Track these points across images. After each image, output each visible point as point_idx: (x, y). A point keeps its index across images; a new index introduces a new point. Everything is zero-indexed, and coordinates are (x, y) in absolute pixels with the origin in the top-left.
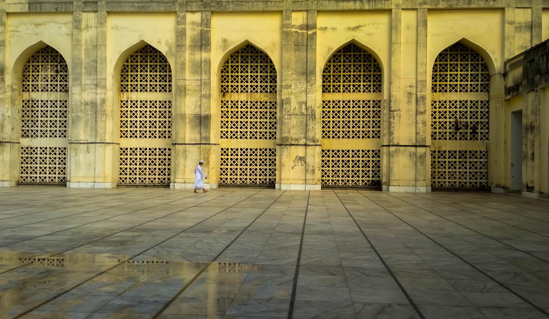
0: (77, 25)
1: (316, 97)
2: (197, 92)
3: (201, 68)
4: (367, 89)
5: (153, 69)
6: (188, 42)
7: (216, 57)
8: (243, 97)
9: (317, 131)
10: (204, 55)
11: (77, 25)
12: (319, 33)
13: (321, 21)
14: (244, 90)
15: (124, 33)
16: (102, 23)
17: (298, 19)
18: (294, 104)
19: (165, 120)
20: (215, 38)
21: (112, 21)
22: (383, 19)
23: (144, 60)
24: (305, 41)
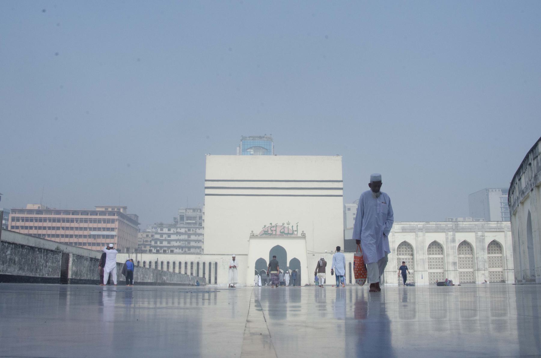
0: (417, 236)
1: (486, 256)
2: (451, 254)
3: (453, 248)
4: (498, 253)
5: (436, 248)
6: (449, 240)
7: (457, 244)
8: (462, 256)
9: (487, 266)
10: (454, 244)
11: (417, 236)
12: (486, 238)
13: (486, 234)
14: (463, 254)
15: (431, 237)
16: (424, 235)
17: (480, 234)
18: (480, 258)
19: (441, 263)
20: (457, 239)
21: (427, 234)
22: (503, 234)
23: (435, 245)
24: (481, 240)
